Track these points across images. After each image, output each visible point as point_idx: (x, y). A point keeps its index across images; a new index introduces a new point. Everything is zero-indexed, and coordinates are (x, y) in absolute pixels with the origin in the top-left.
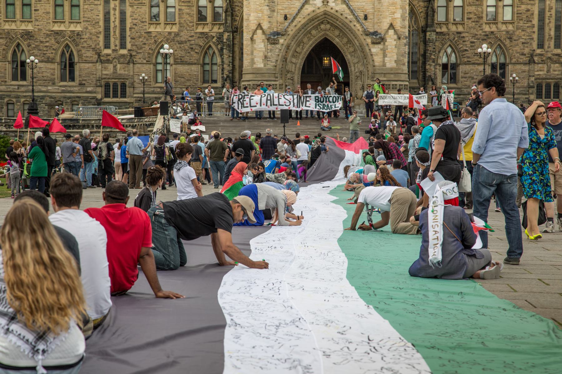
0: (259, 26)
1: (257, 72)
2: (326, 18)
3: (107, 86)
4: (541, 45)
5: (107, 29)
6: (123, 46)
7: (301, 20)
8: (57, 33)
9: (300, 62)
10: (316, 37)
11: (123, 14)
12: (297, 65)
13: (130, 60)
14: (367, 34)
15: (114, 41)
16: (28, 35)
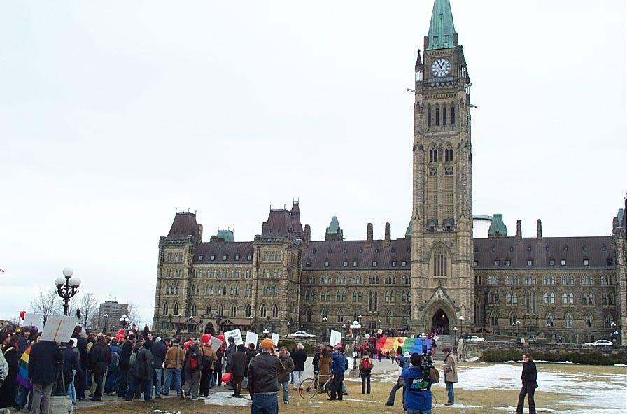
0: (416, 305)
1: (416, 320)
2: (440, 302)
3: (370, 324)
4: (528, 312)
5: (370, 304)
6: (376, 310)
7: (430, 303)
8: (353, 305)
9: (431, 317)
10: (437, 308)
11: (376, 298)
12: (430, 319)
13: (378, 315)
14: (454, 307)
15: (373, 308)
16: (344, 306)
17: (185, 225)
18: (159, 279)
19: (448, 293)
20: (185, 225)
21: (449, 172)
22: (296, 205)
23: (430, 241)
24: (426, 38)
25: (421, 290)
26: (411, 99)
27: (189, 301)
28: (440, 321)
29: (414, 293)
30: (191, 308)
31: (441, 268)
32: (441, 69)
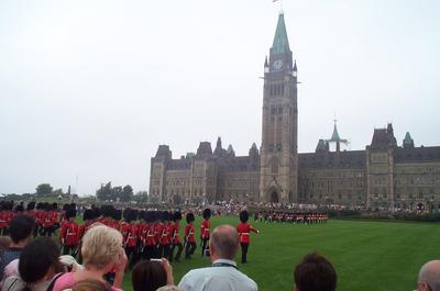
17: (164, 151)
18: (151, 178)
19: (279, 183)
20: (164, 151)
21: (280, 119)
22: (219, 139)
23: (269, 156)
24: (271, 50)
25: (265, 181)
26: (262, 82)
27: (163, 188)
28: (275, 197)
29: (262, 183)
30: (164, 192)
31: (275, 170)
32: (278, 65)
